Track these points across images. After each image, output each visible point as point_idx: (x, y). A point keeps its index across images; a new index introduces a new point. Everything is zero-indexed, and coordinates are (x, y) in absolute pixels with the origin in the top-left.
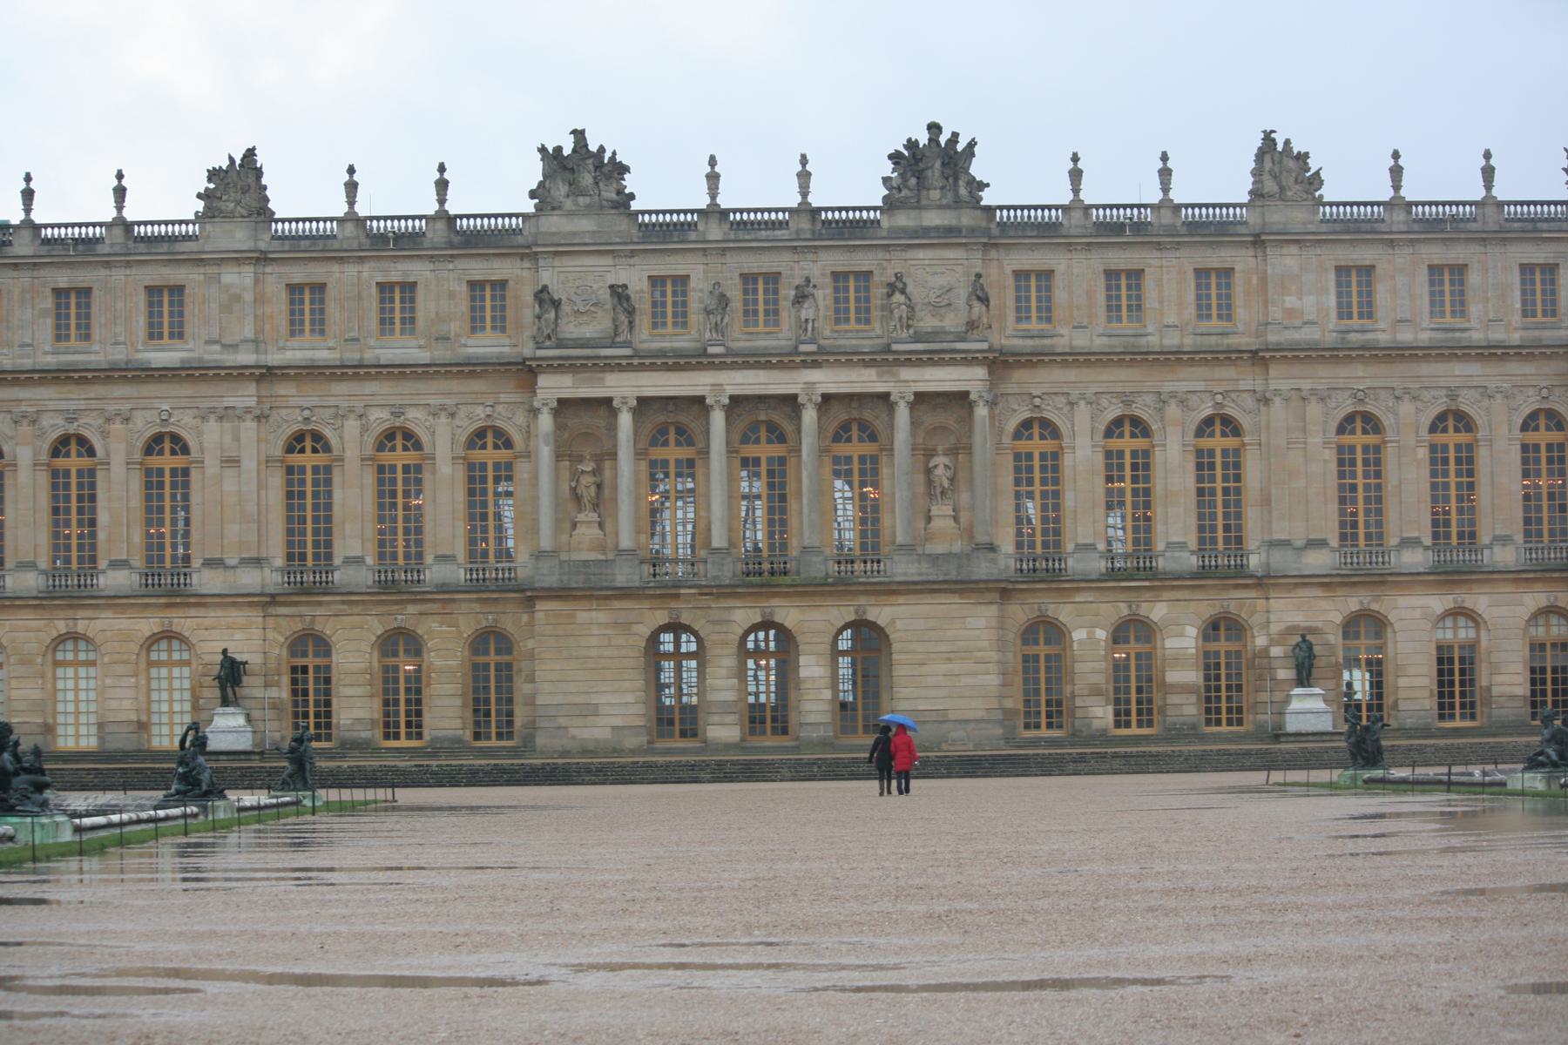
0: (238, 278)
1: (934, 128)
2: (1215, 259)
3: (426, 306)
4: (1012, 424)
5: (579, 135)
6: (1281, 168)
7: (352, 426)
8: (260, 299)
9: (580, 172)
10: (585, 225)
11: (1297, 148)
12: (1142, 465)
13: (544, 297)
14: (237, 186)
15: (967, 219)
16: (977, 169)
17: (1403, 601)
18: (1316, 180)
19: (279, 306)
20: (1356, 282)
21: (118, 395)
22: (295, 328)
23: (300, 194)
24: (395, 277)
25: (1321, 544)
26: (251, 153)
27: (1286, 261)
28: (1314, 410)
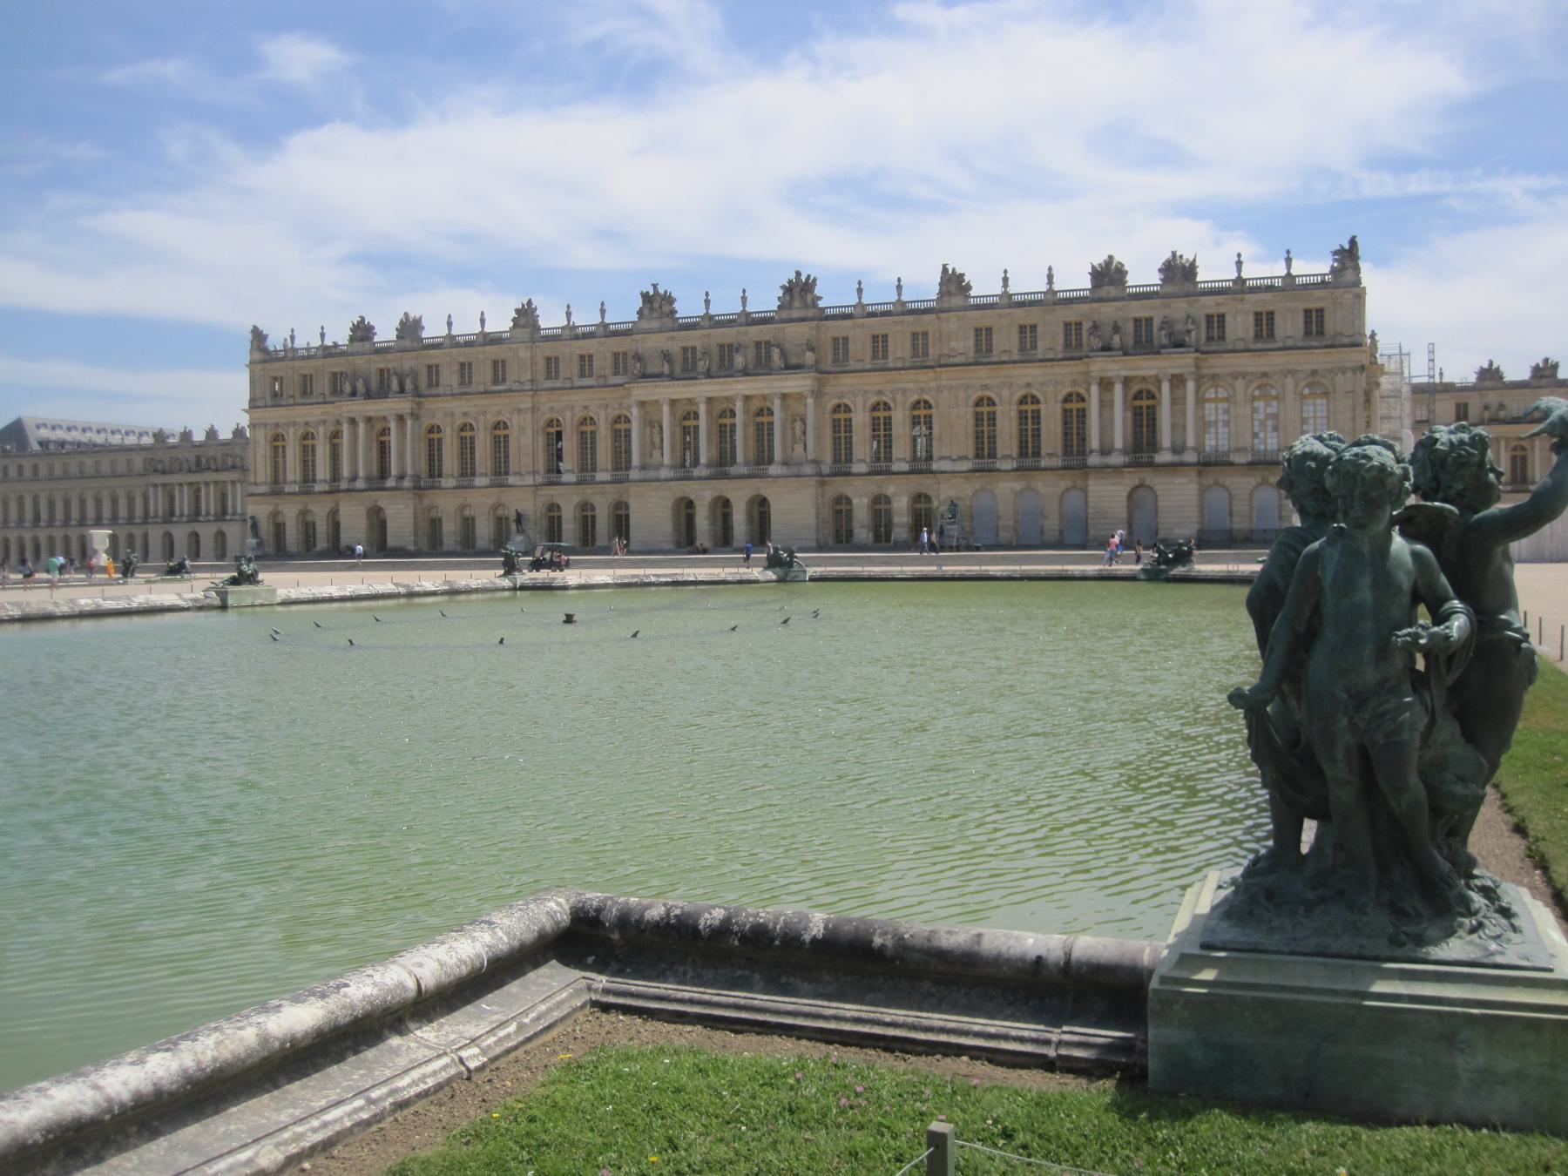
0: (524, 353)
1: (798, 274)
2: (919, 329)
3: (596, 362)
4: (830, 406)
5: (655, 286)
6: (953, 283)
7: (568, 415)
8: (533, 363)
9: (656, 304)
10: (655, 324)
11: (959, 271)
12: (888, 422)
13: (638, 357)
14: (526, 316)
15: (811, 313)
16: (817, 291)
17: (1001, 485)
18: (969, 287)
19: (541, 367)
20: (983, 336)
21: (482, 401)
22: (549, 377)
23: (550, 319)
24: (584, 352)
25: (966, 458)
26: (530, 302)
27: (952, 323)
28: (962, 395)
